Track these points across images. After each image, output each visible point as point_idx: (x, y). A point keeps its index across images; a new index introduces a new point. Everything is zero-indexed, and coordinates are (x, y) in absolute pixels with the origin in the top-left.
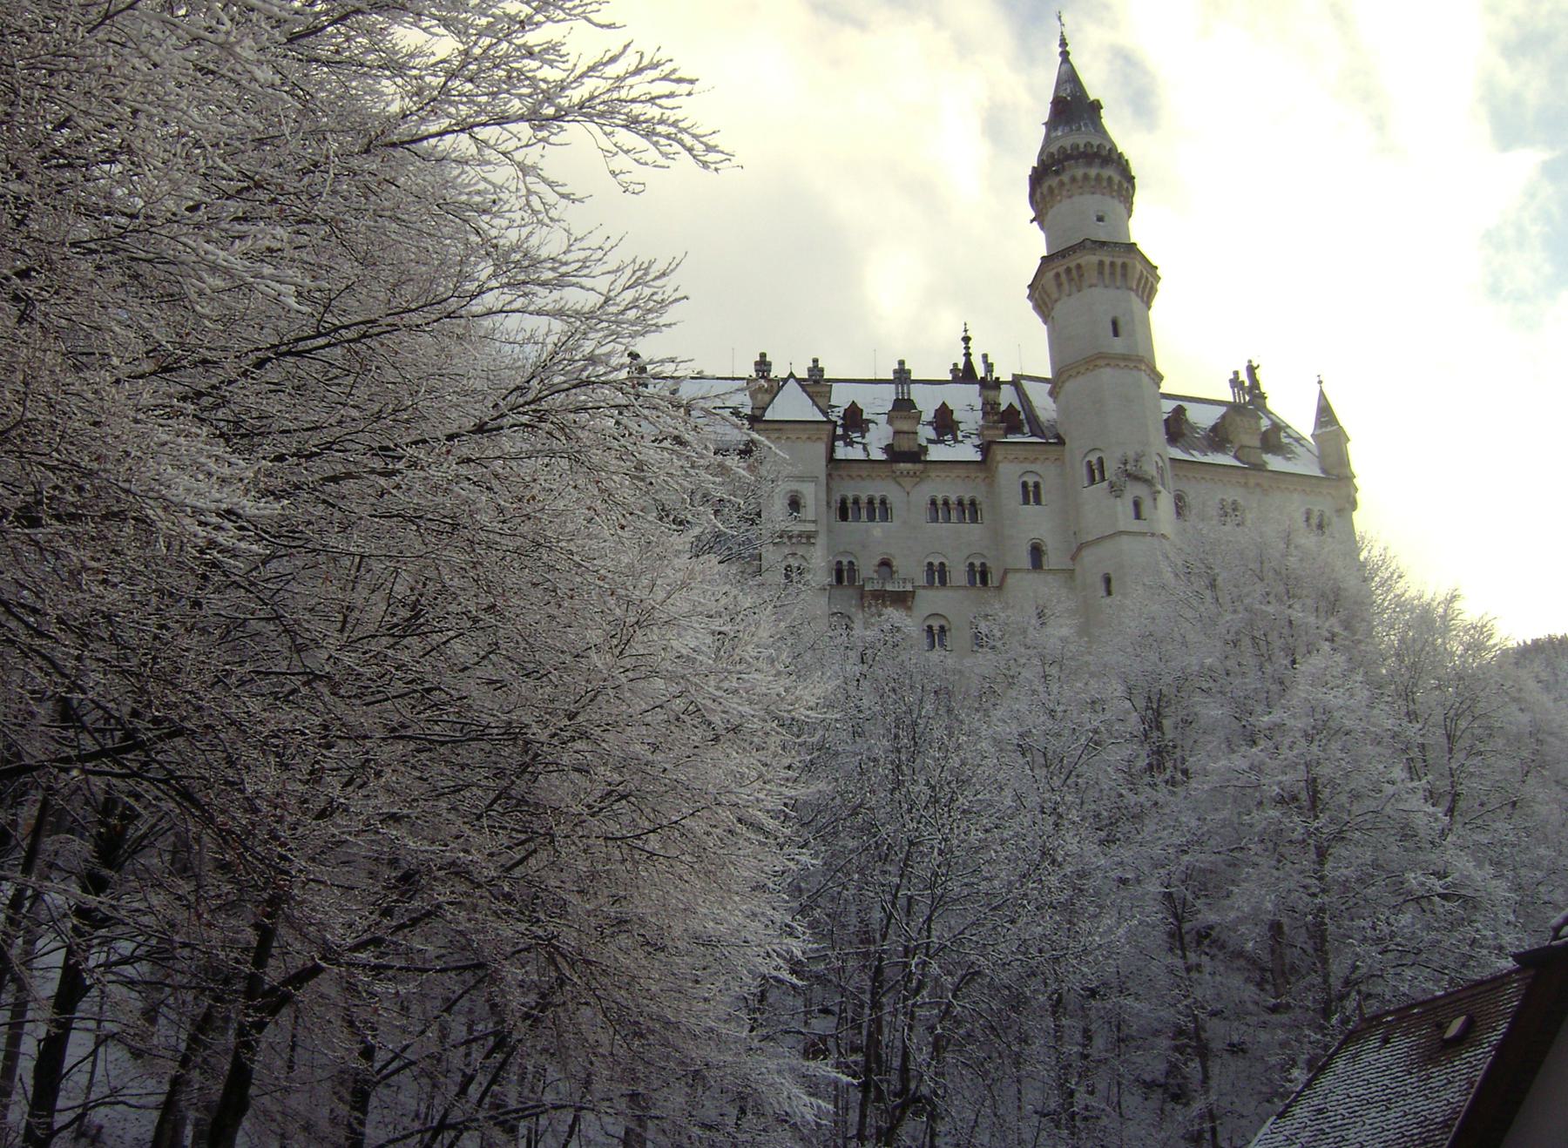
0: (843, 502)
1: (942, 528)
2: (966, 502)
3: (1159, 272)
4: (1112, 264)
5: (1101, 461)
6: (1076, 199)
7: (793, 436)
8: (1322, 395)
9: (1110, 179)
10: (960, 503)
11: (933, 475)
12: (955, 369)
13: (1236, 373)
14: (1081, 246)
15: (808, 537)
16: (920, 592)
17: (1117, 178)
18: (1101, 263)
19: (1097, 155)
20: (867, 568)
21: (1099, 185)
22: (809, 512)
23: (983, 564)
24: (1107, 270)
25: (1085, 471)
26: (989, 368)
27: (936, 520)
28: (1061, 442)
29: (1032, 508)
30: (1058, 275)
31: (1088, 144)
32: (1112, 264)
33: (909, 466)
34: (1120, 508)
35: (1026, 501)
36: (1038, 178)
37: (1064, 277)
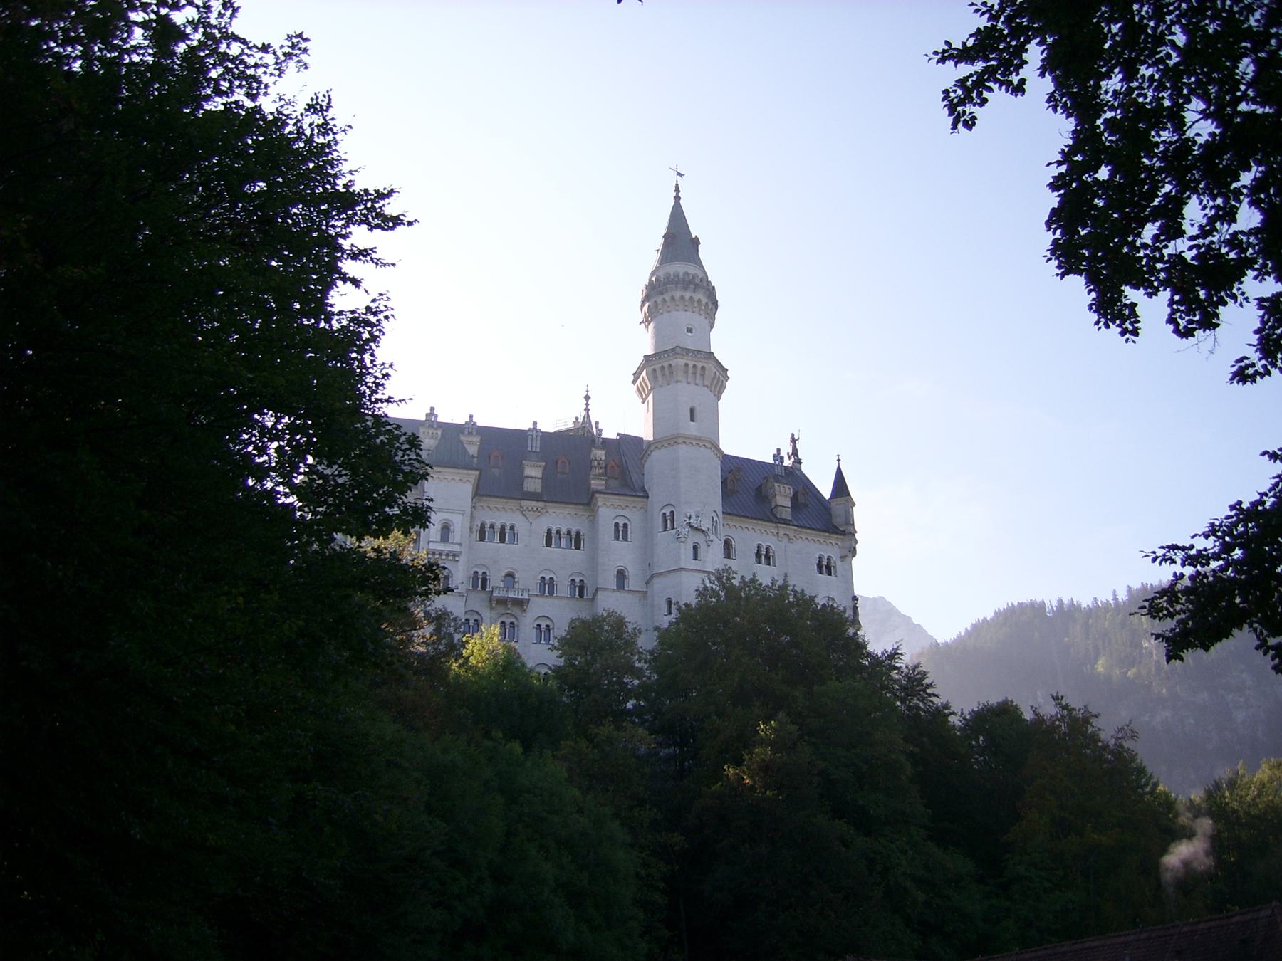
0: (483, 526)
1: (553, 550)
2: (573, 533)
3: (729, 374)
4: (695, 366)
5: (672, 512)
8: (839, 468)
9: (699, 301)
10: (569, 533)
13: (779, 450)
14: (675, 352)
16: (533, 599)
17: (704, 300)
18: (687, 365)
19: (691, 282)
20: (496, 580)
22: (456, 536)
24: (691, 370)
25: (660, 519)
29: (621, 543)
32: (695, 366)
33: (534, 503)
34: (682, 551)
35: (617, 538)
37: (659, 372)
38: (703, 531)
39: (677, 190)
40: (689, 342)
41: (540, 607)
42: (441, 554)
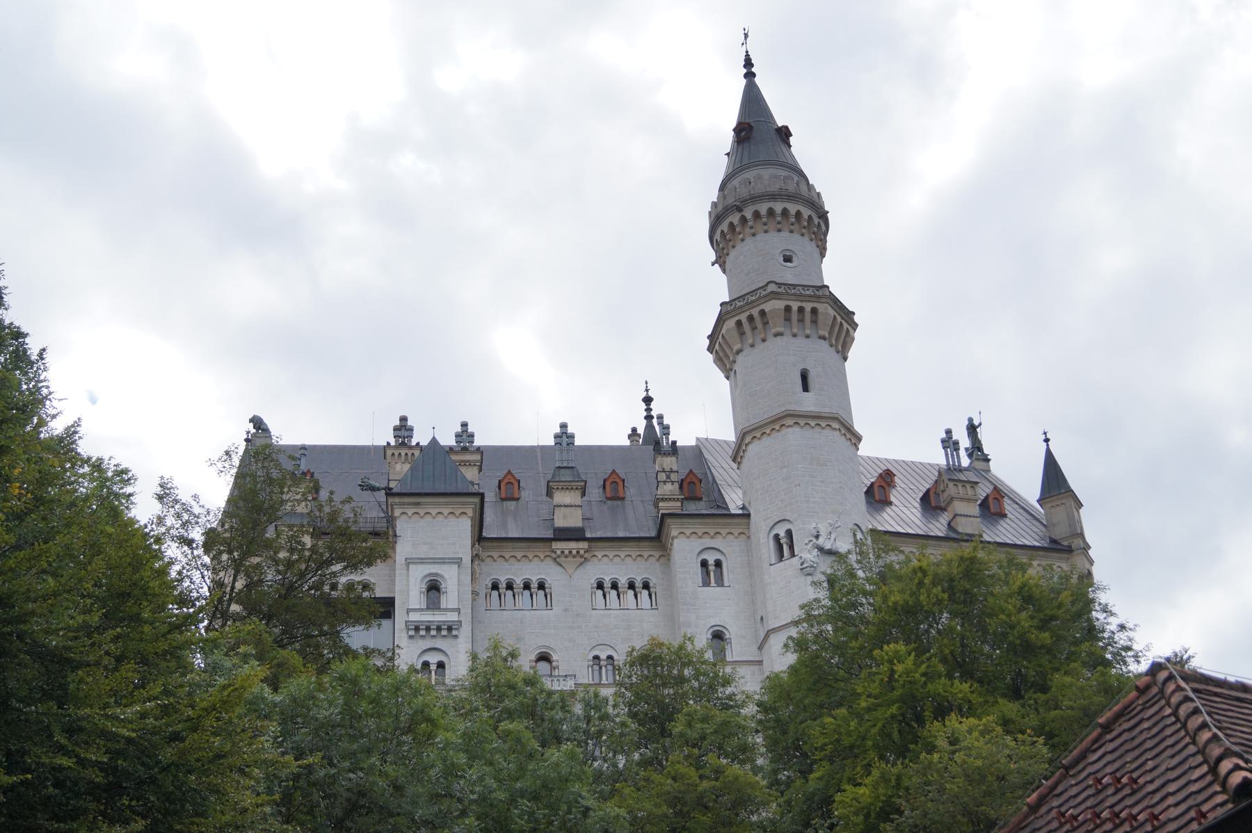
3: (856, 319)
4: (801, 310)
5: (789, 533)
6: (761, 237)
7: (434, 511)
9: (798, 214)
11: (599, 554)
12: (634, 433)
13: (949, 432)
15: (450, 629)
17: (806, 212)
18: (788, 309)
22: (450, 598)
24: (795, 316)
25: (772, 543)
26: (666, 429)
28: (747, 516)
29: (713, 590)
30: (739, 323)
32: (801, 310)
33: (573, 545)
35: (706, 583)
36: (717, 218)
39: (748, 63)
40: (789, 275)
42: (428, 629)
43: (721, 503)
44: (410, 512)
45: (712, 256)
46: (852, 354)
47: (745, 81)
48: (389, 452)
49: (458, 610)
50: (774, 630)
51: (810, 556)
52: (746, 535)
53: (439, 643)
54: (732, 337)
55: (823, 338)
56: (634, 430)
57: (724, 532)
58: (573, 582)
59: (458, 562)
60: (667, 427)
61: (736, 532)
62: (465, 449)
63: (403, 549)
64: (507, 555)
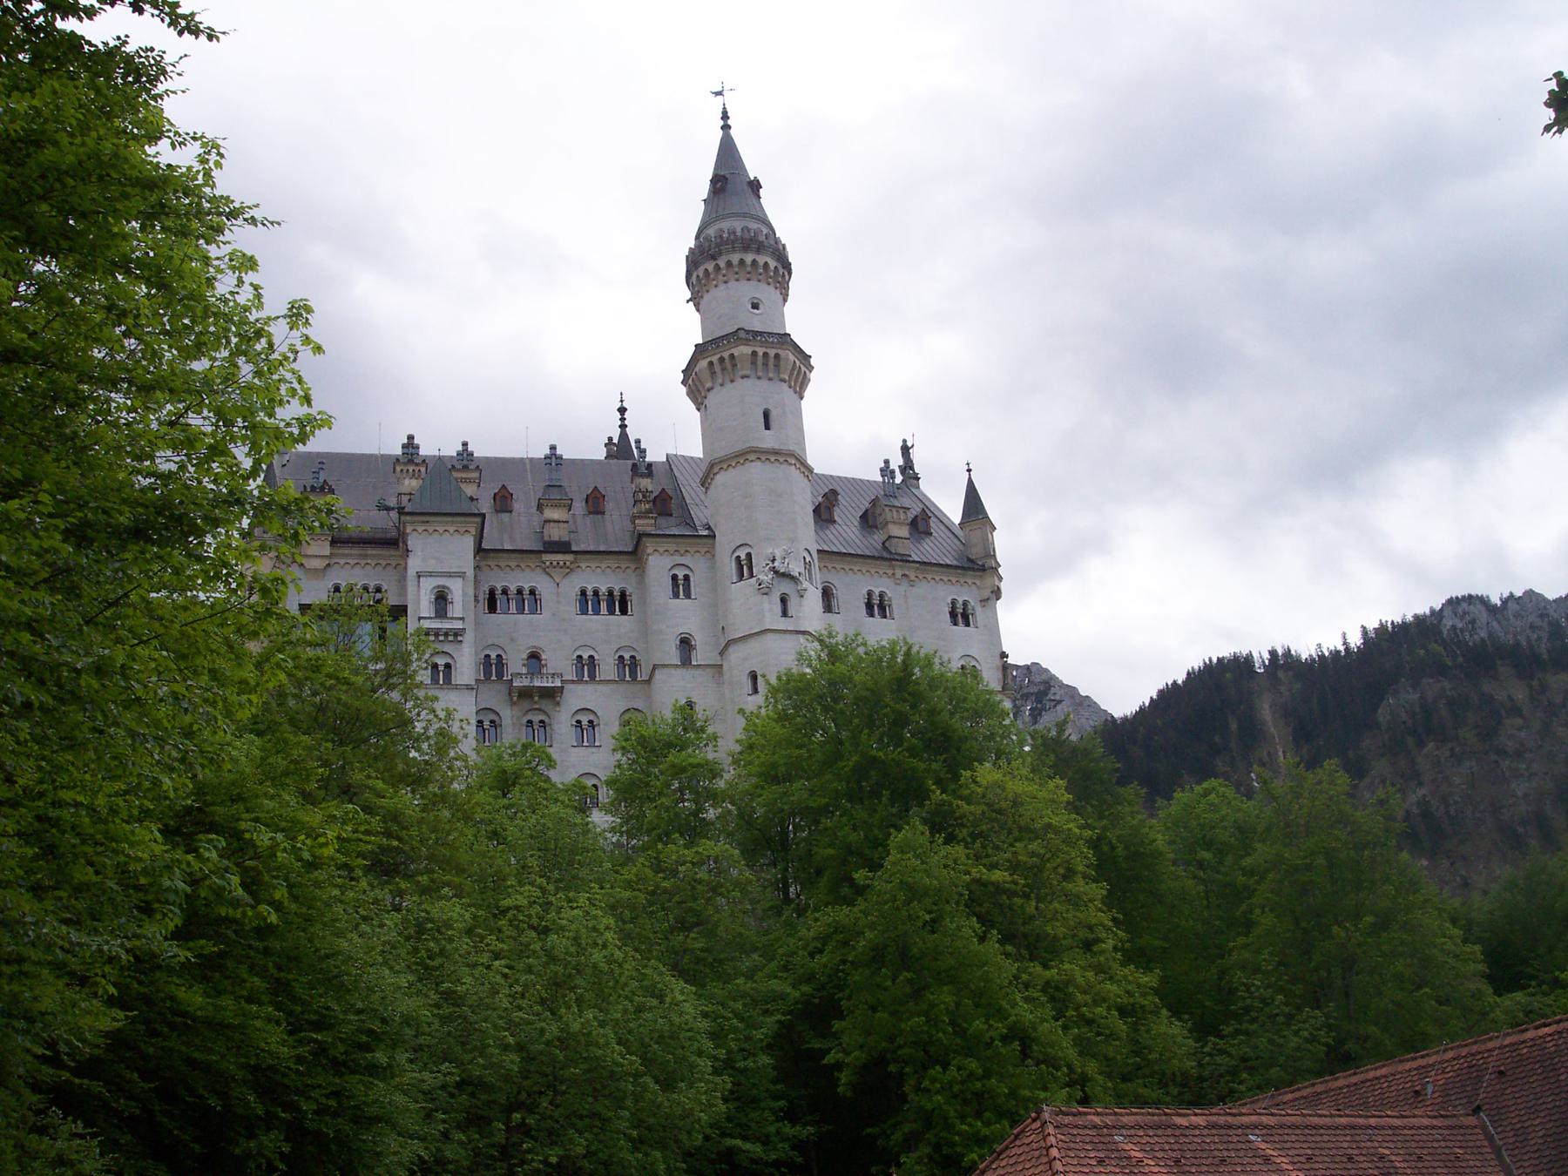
0: (492, 593)
1: (591, 620)
3: (812, 361)
4: (765, 354)
5: (749, 555)
6: (732, 284)
7: (441, 529)
10: (611, 593)
11: (583, 565)
13: (887, 462)
14: (737, 336)
16: (568, 687)
17: (772, 264)
18: (754, 353)
20: (516, 663)
21: (753, 272)
22: (456, 610)
23: (633, 657)
25: (733, 564)
26: (643, 452)
27: (584, 612)
29: (682, 602)
30: (711, 363)
31: (746, 229)
32: (765, 354)
33: (560, 557)
35: (676, 596)
36: (694, 261)
37: (717, 367)
38: (793, 578)
41: (579, 697)
42: (437, 635)
43: (688, 521)
44: (420, 529)
45: (689, 295)
46: (809, 392)
47: (719, 134)
48: (398, 469)
49: (462, 619)
50: (735, 641)
51: (766, 577)
52: (711, 553)
53: (447, 648)
54: (705, 373)
55: (783, 380)
56: (610, 439)
57: (692, 550)
58: (559, 592)
59: (462, 575)
60: (644, 451)
61: (703, 550)
62: (465, 468)
63: (414, 564)
64: (502, 564)
